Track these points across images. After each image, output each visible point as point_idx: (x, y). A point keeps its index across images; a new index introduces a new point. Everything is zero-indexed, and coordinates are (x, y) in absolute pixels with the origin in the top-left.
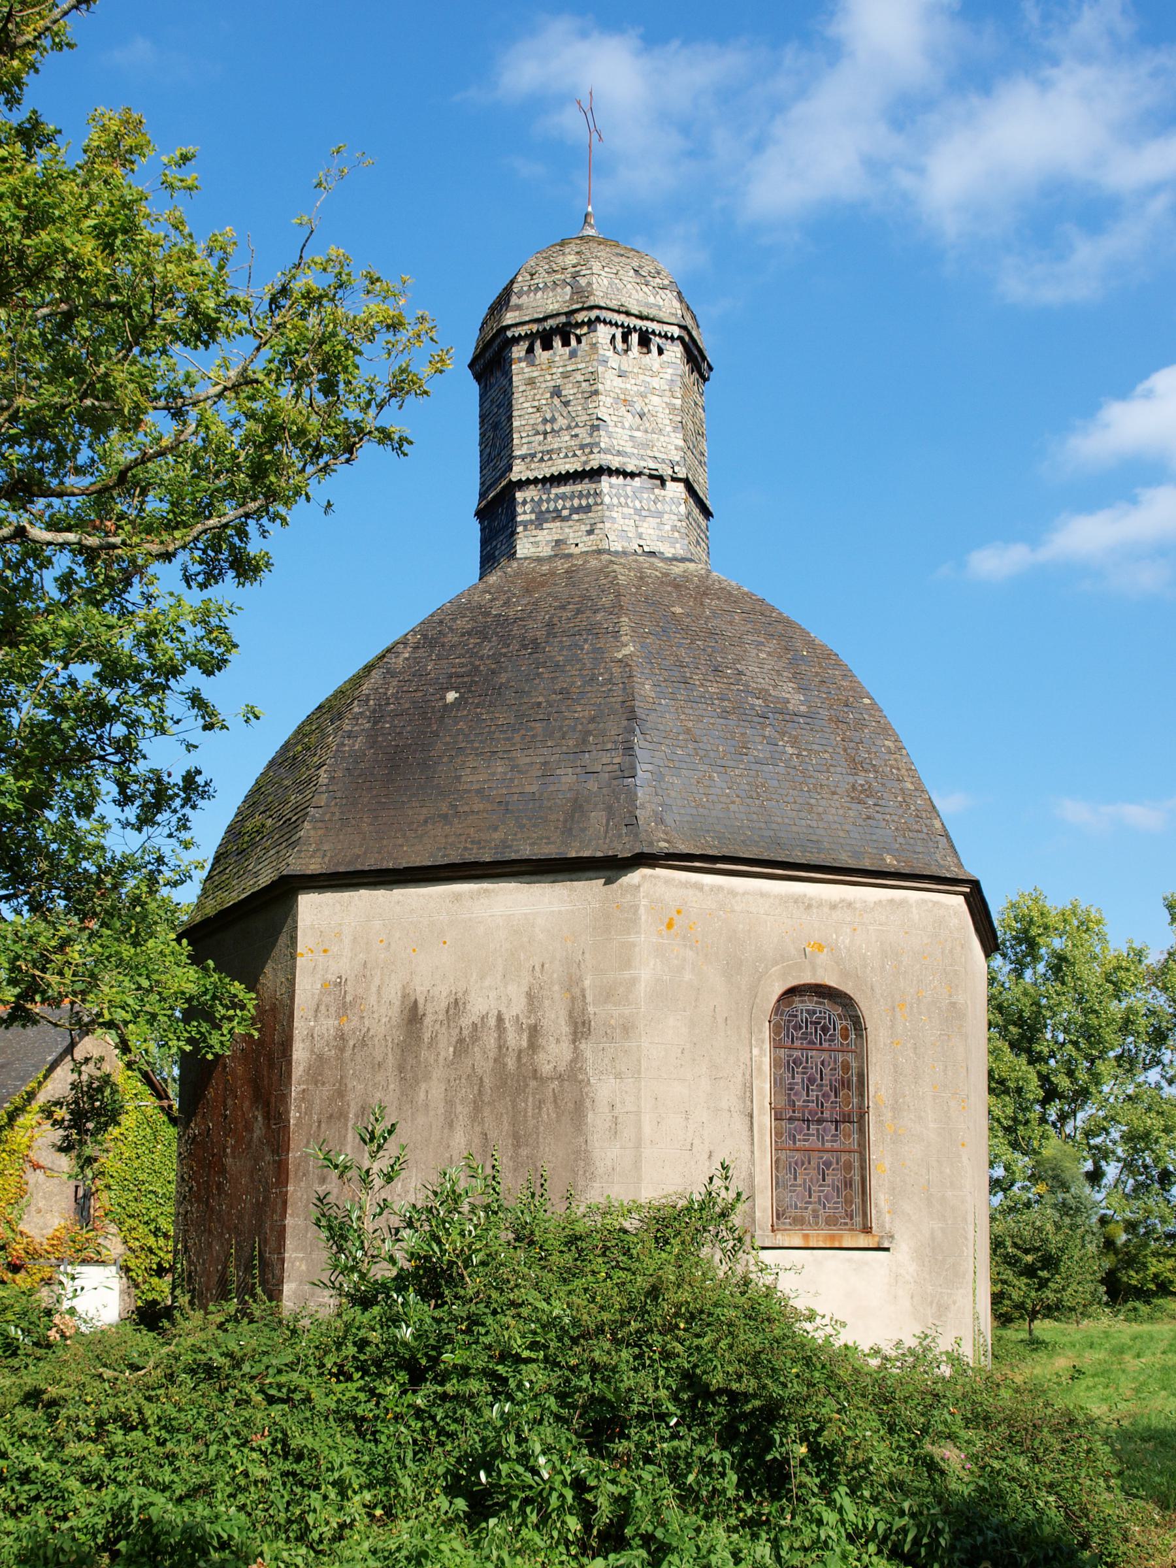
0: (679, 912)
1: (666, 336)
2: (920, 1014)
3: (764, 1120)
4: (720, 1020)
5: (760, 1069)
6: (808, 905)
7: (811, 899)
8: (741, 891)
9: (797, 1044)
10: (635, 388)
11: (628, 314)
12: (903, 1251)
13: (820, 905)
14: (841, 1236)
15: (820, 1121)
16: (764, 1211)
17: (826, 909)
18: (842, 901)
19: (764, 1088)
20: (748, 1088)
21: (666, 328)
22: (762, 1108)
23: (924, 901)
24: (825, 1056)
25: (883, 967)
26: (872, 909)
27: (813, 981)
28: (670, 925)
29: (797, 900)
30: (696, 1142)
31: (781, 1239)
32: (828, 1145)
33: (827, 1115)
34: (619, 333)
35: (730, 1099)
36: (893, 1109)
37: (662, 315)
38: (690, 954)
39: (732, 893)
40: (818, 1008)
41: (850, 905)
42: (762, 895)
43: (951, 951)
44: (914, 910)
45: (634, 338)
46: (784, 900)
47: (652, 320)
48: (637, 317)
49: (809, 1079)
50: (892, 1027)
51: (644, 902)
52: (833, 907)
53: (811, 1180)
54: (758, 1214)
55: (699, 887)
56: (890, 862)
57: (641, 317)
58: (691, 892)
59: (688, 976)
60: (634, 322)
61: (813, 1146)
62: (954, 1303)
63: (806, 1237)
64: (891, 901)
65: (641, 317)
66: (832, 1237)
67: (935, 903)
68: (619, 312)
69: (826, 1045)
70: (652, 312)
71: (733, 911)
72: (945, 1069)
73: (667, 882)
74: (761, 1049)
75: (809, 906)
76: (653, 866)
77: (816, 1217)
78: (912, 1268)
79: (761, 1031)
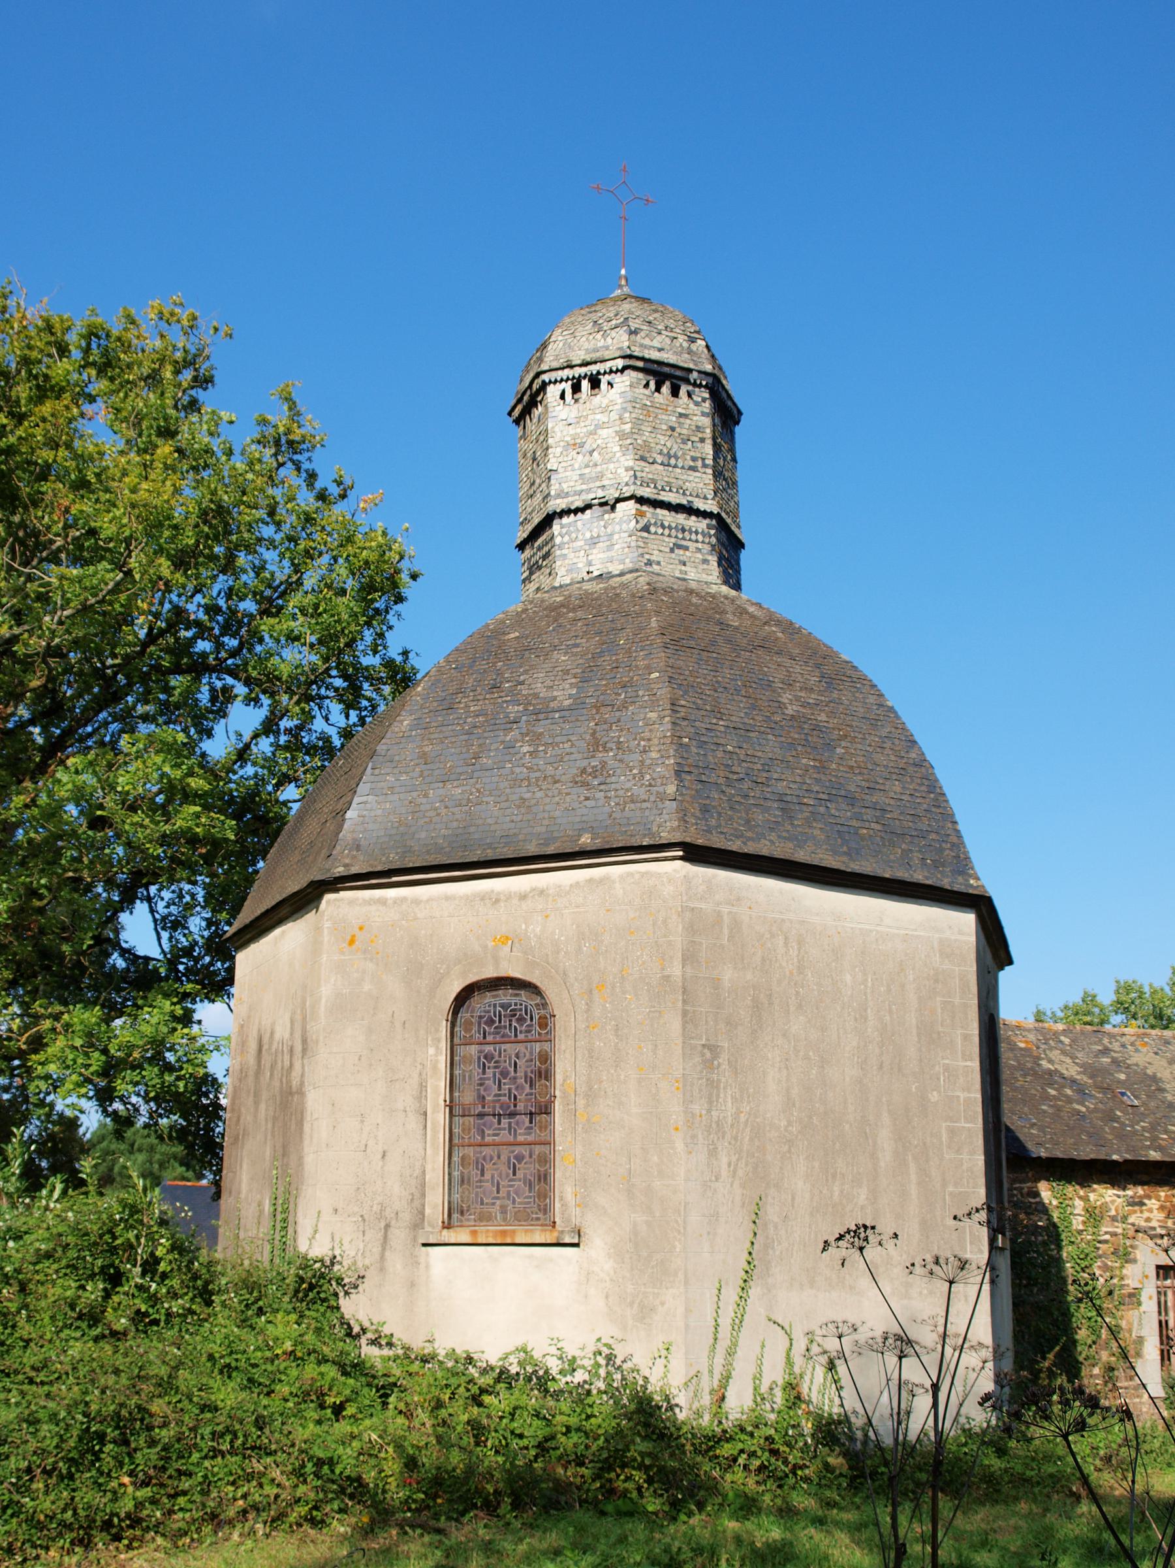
0: (361, 928)
1: (611, 371)
2: (624, 993)
3: (439, 1117)
4: (398, 1025)
5: (435, 1067)
6: (496, 900)
7: (498, 894)
8: (425, 898)
9: (489, 1038)
10: (585, 430)
11: (571, 367)
12: (597, 1247)
13: (509, 897)
14: (514, 1232)
15: (512, 1115)
16: (435, 1206)
17: (515, 901)
18: (533, 890)
19: (438, 1086)
20: (422, 1087)
21: (609, 364)
22: (436, 1105)
23: (630, 874)
24: (520, 1047)
25: (579, 950)
26: (568, 893)
27: (495, 975)
28: (352, 942)
29: (483, 897)
30: (371, 1143)
31: (448, 1236)
32: (521, 1138)
33: (521, 1107)
34: (567, 387)
35: (405, 1099)
36: (587, 1096)
37: (607, 354)
38: (370, 966)
39: (417, 902)
40: (514, 1000)
41: (542, 892)
42: (447, 898)
43: (665, 922)
44: (617, 885)
45: (585, 384)
46: (469, 899)
47: (595, 363)
48: (581, 365)
49: (502, 1073)
50: (587, 1011)
51: (327, 925)
52: (523, 897)
53: (500, 1175)
54: (428, 1211)
55: (383, 902)
56: (586, 841)
57: (585, 364)
58: (373, 908)
59: (367, 987)
60: (578, 371)
61: (505, 1140)
62: (663, 1304)
63: (474, 1233)
64: (590, 881)
65: (585, 364)
66: (504, 1233)
67: (643, 875)
68: (563, 368)
69: (521, 1037)
70: (595, 356)
71: (416, 919)
72: (654, 1051)
73: (351, 902)
74: (437, 1048)
75: (497, 901)
76: (337, 890)
77: (503, 1210)
78: (608, 1265)
79: (437, 1030)
